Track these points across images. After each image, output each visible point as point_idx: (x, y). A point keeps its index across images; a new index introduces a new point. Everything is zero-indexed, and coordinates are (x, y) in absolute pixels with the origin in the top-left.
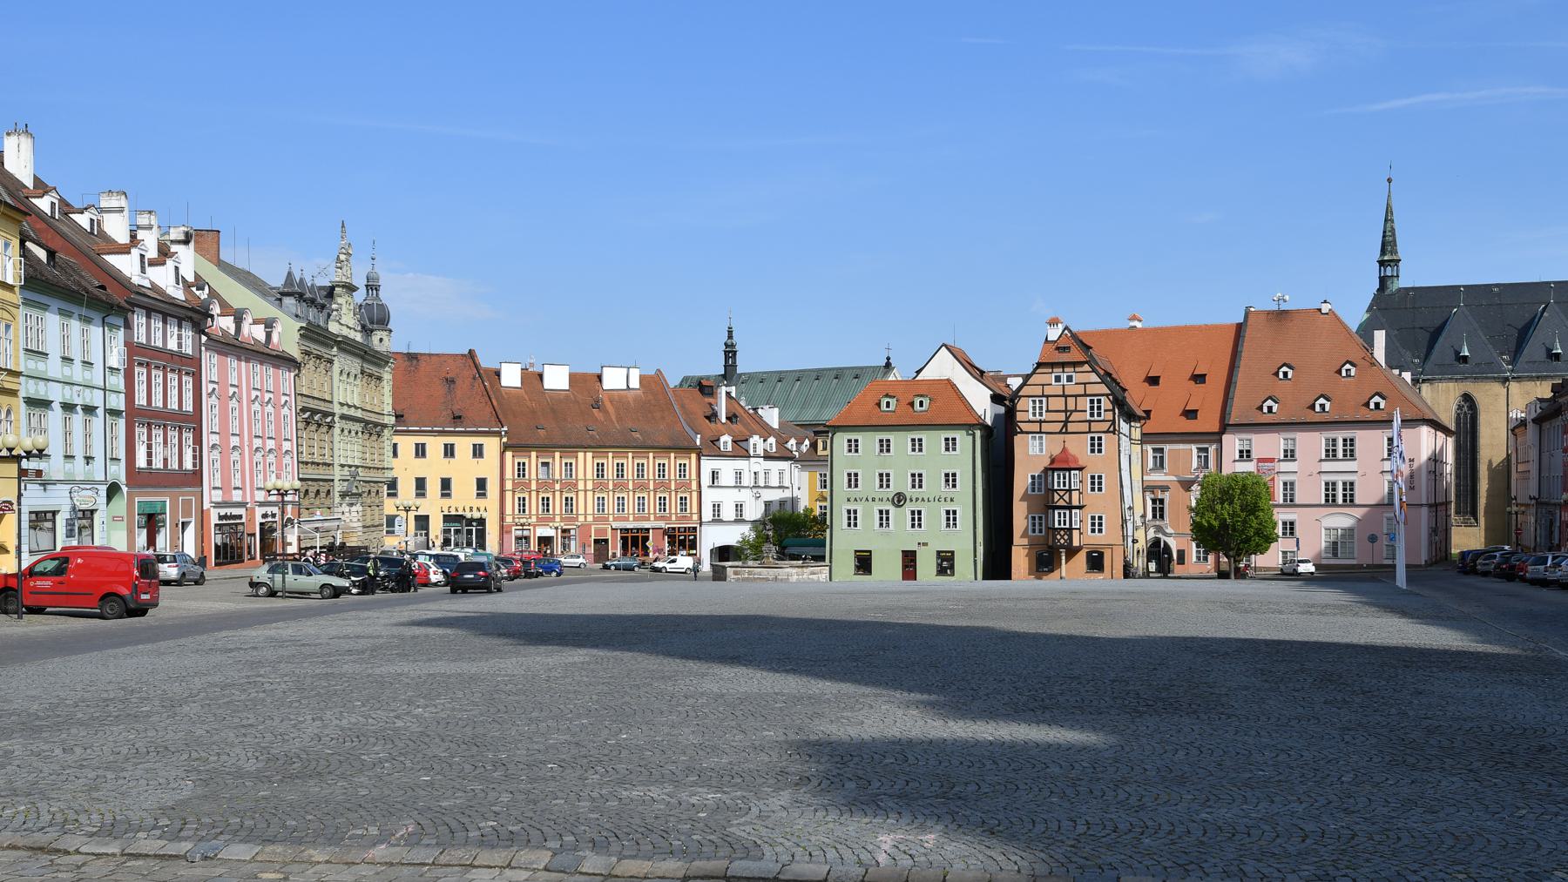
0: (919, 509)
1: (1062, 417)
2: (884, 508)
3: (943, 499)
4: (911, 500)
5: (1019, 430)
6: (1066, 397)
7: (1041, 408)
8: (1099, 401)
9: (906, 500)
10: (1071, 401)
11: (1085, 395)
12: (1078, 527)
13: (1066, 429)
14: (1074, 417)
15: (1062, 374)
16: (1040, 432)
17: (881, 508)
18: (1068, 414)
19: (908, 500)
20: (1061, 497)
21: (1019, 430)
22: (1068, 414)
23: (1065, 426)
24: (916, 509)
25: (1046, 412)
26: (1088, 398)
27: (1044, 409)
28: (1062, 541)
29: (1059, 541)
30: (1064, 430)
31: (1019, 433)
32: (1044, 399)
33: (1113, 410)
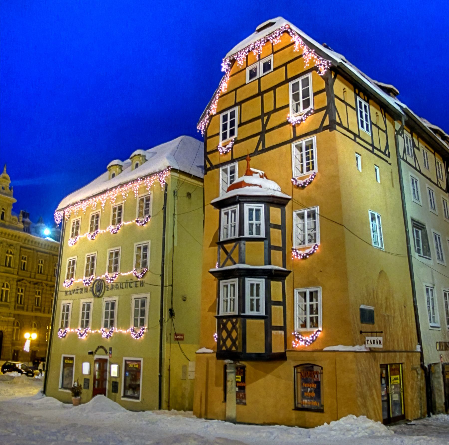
1: (257, 126)
5: (209, 166)
7: (232, 123)
8: (306, 83)
10: (269, 96)
11: (288, 81)
12: (262, 312)
13: (264, 145)
14: (274, 120)
15: (257, 65)
16: (233, 161)
18: (265, 118)
21: (209, 166)
22: (265, 118)
23: (262, 140)
25: (239, 126)
26: (290, 84)
27: (237, 123)
28: (229, 343)
29: (224, 342)
30: (260, 148)
31: (209, 169)
32: (237, 109)
33: (329, 89)
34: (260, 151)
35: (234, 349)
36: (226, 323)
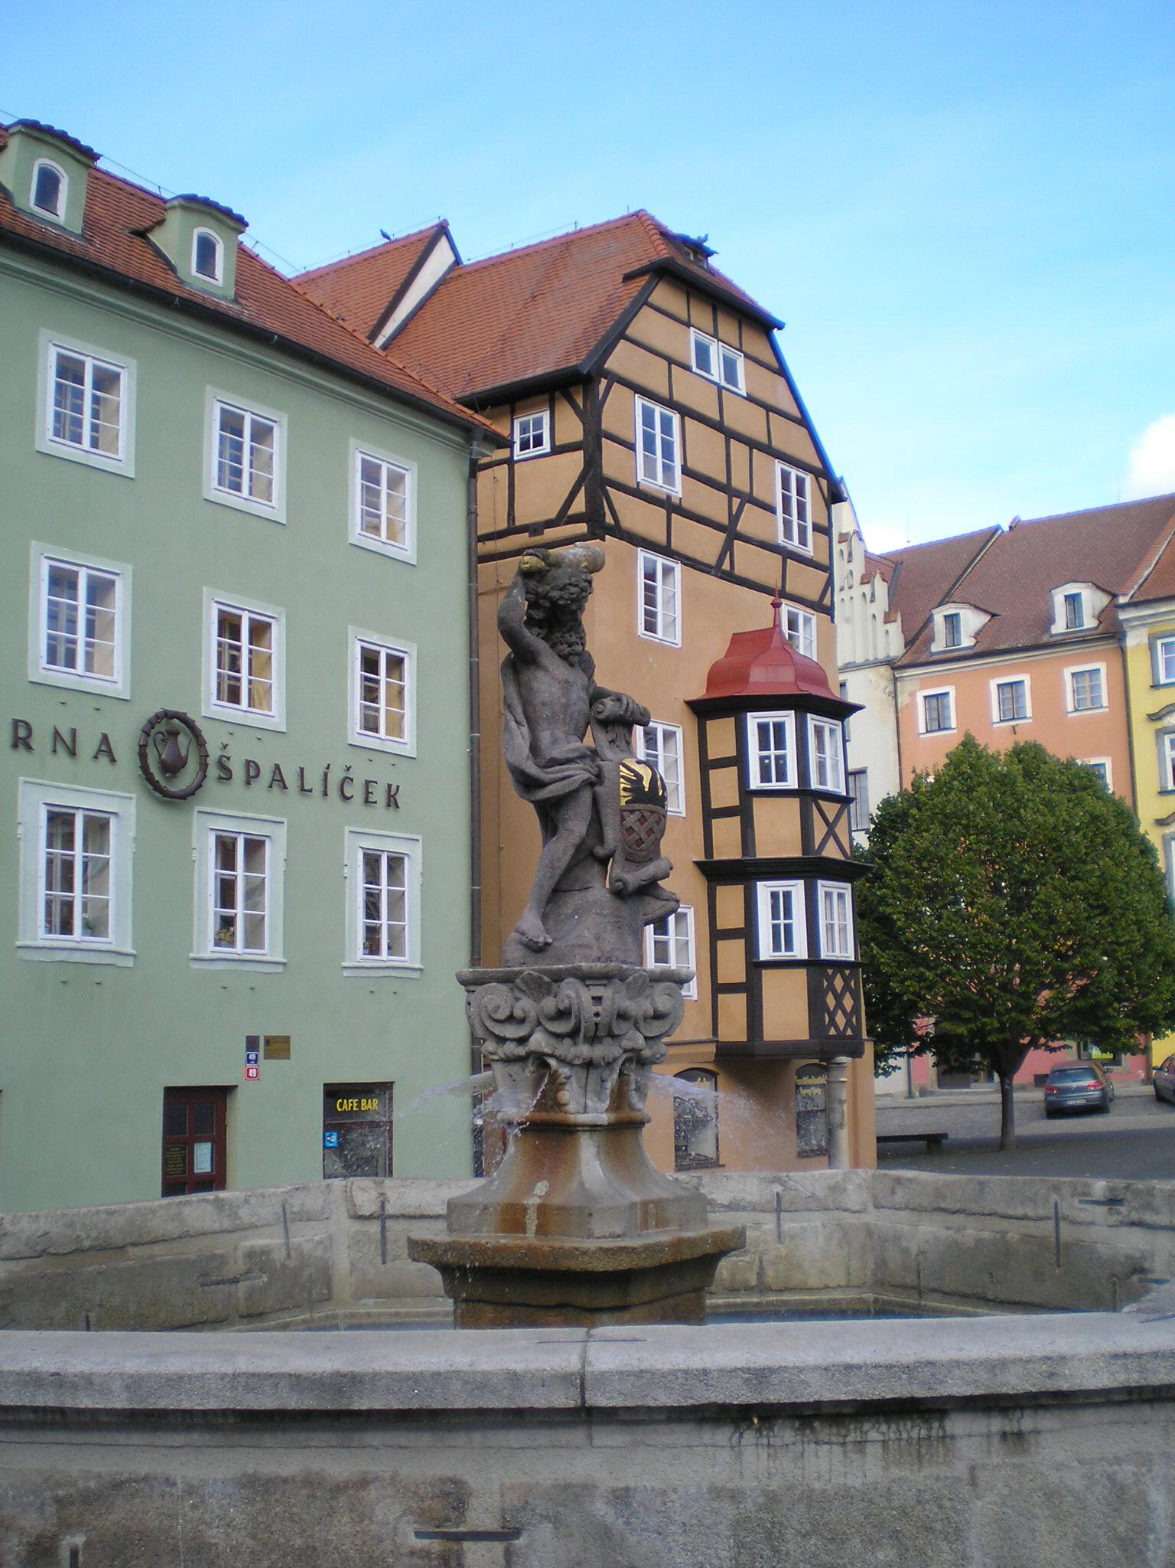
0: (256, 830)
2: (82, 800)
3: (355, 790)
4: (226, 775)
5: (609, 519)
6: (730, 435)
9: (204, 766)
11: (769, 450)
17: (66, 799)
19: (213, 771)
20: (831, 827)
24: (242, 829)
26: (779, 466)
28: (840, 1020)
29: (832, 1016)
30: (726, 566)
34: (724, 572)
35: (849, 1032)
36: (833, 976)
